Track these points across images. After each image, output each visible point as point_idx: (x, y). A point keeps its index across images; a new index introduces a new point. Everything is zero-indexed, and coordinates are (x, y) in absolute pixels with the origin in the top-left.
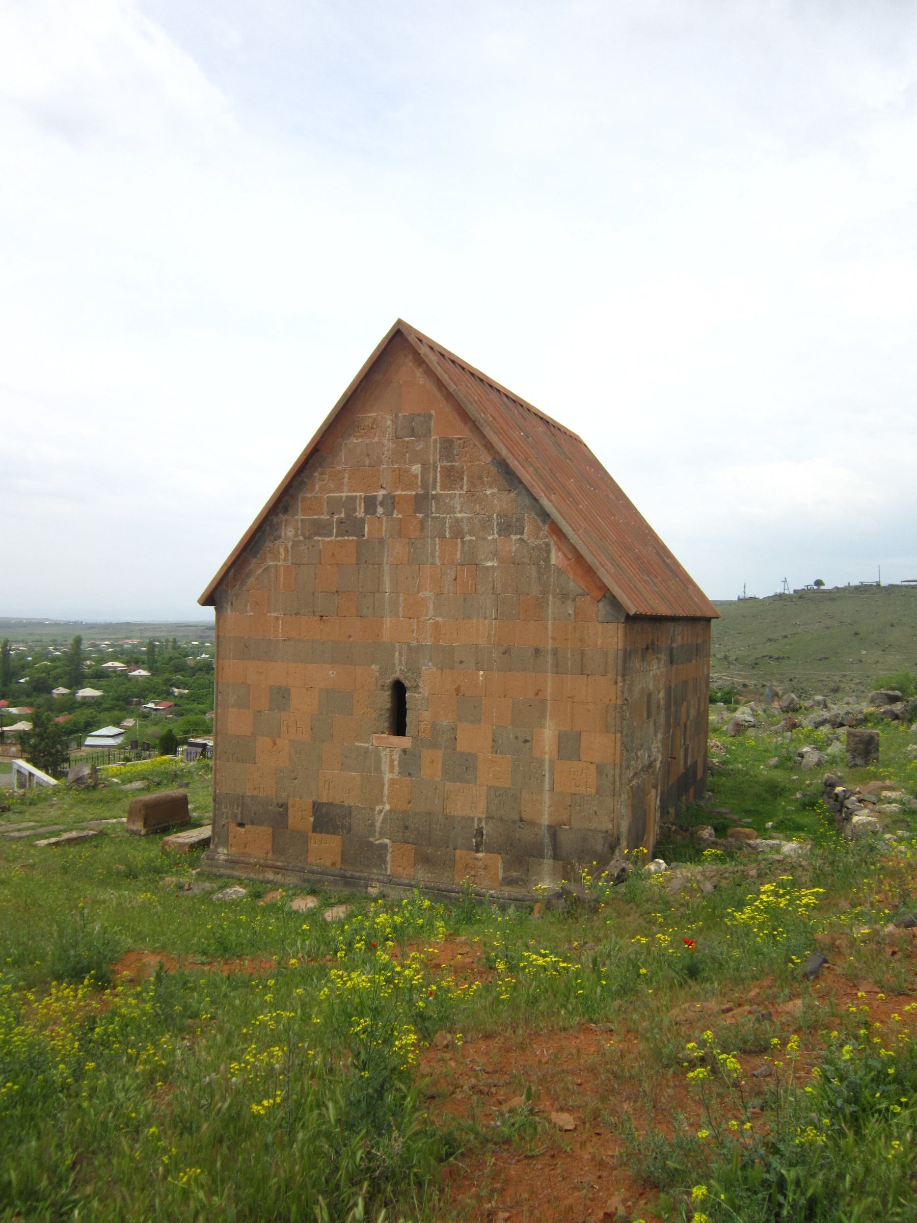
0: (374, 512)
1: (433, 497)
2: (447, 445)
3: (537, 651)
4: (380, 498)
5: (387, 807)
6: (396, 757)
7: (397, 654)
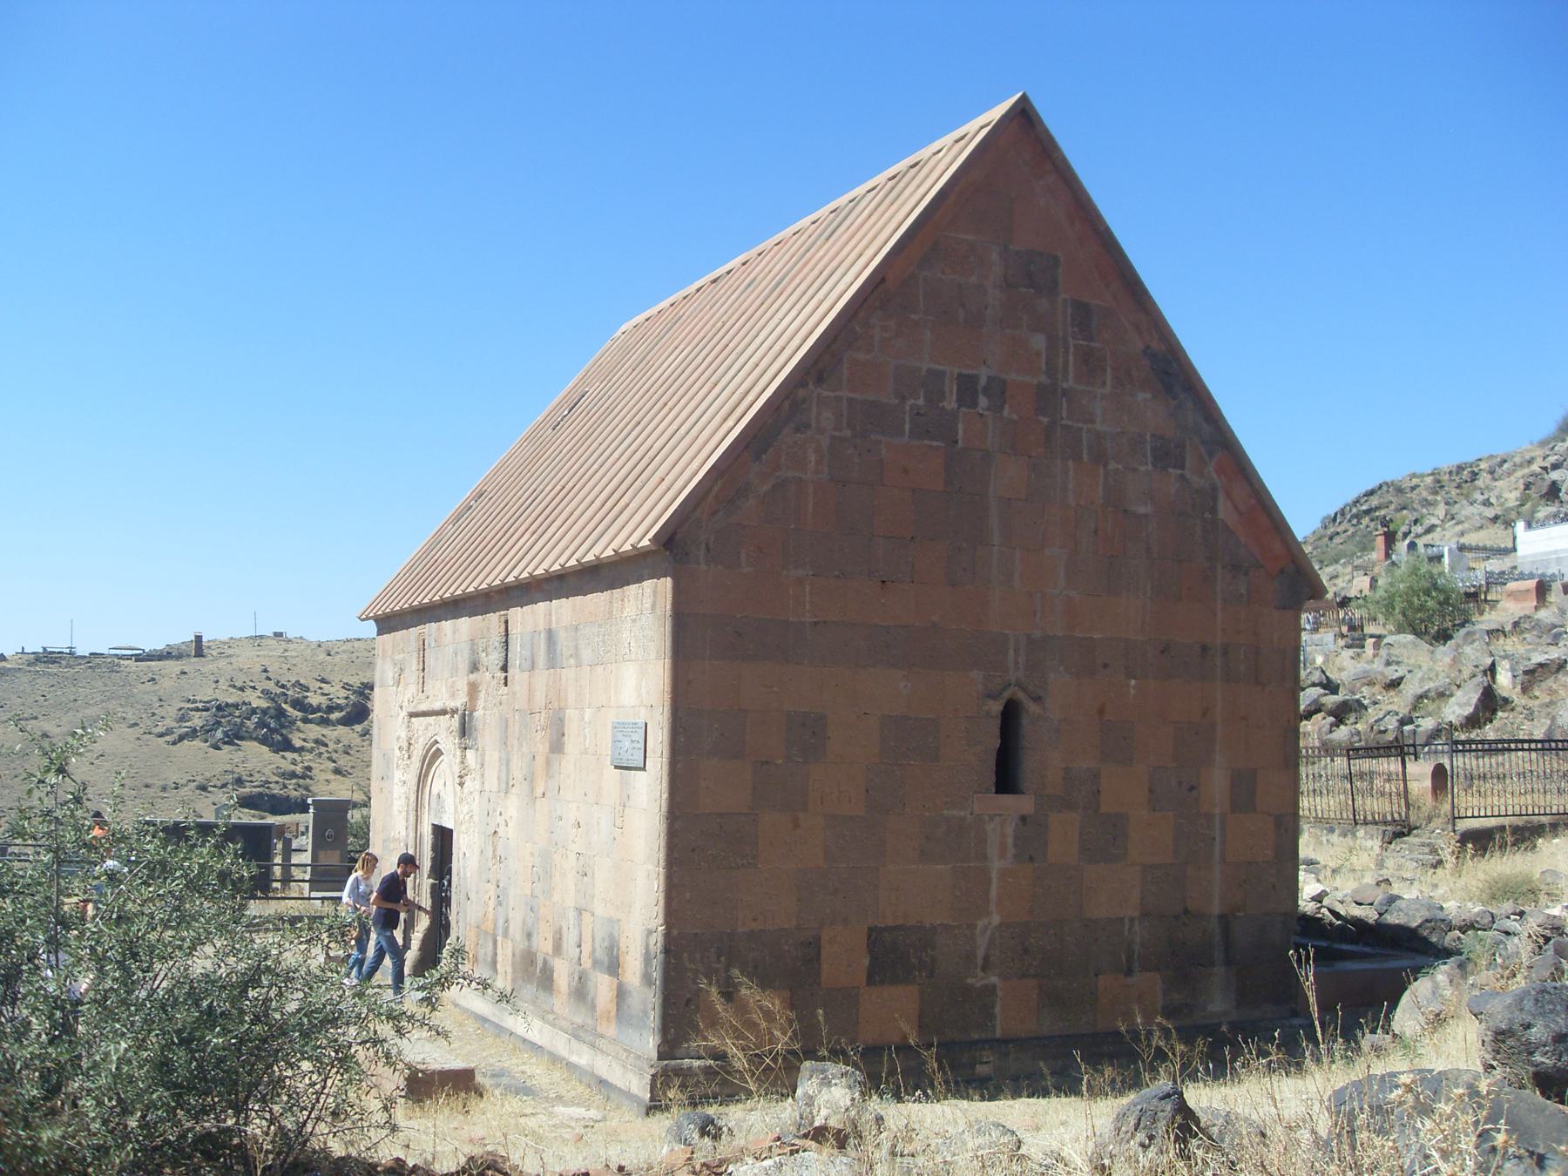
0: (974, 404)
1: (1065, 393)
2: (1082, 314)
3: (1204, 649)
4: (983, 382)
5: (996, 920)
6: (1010, 830)
7: (1011, 652)
